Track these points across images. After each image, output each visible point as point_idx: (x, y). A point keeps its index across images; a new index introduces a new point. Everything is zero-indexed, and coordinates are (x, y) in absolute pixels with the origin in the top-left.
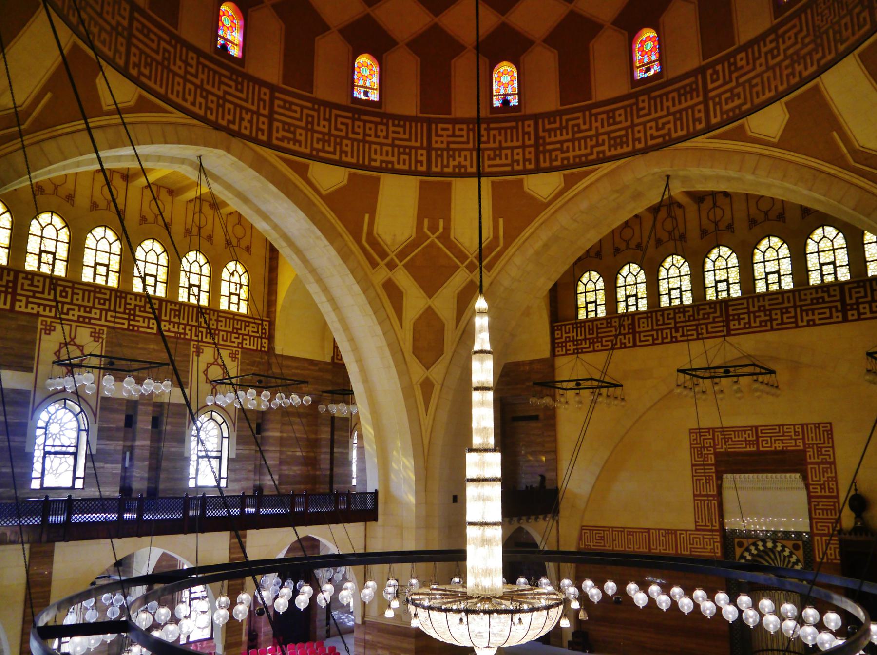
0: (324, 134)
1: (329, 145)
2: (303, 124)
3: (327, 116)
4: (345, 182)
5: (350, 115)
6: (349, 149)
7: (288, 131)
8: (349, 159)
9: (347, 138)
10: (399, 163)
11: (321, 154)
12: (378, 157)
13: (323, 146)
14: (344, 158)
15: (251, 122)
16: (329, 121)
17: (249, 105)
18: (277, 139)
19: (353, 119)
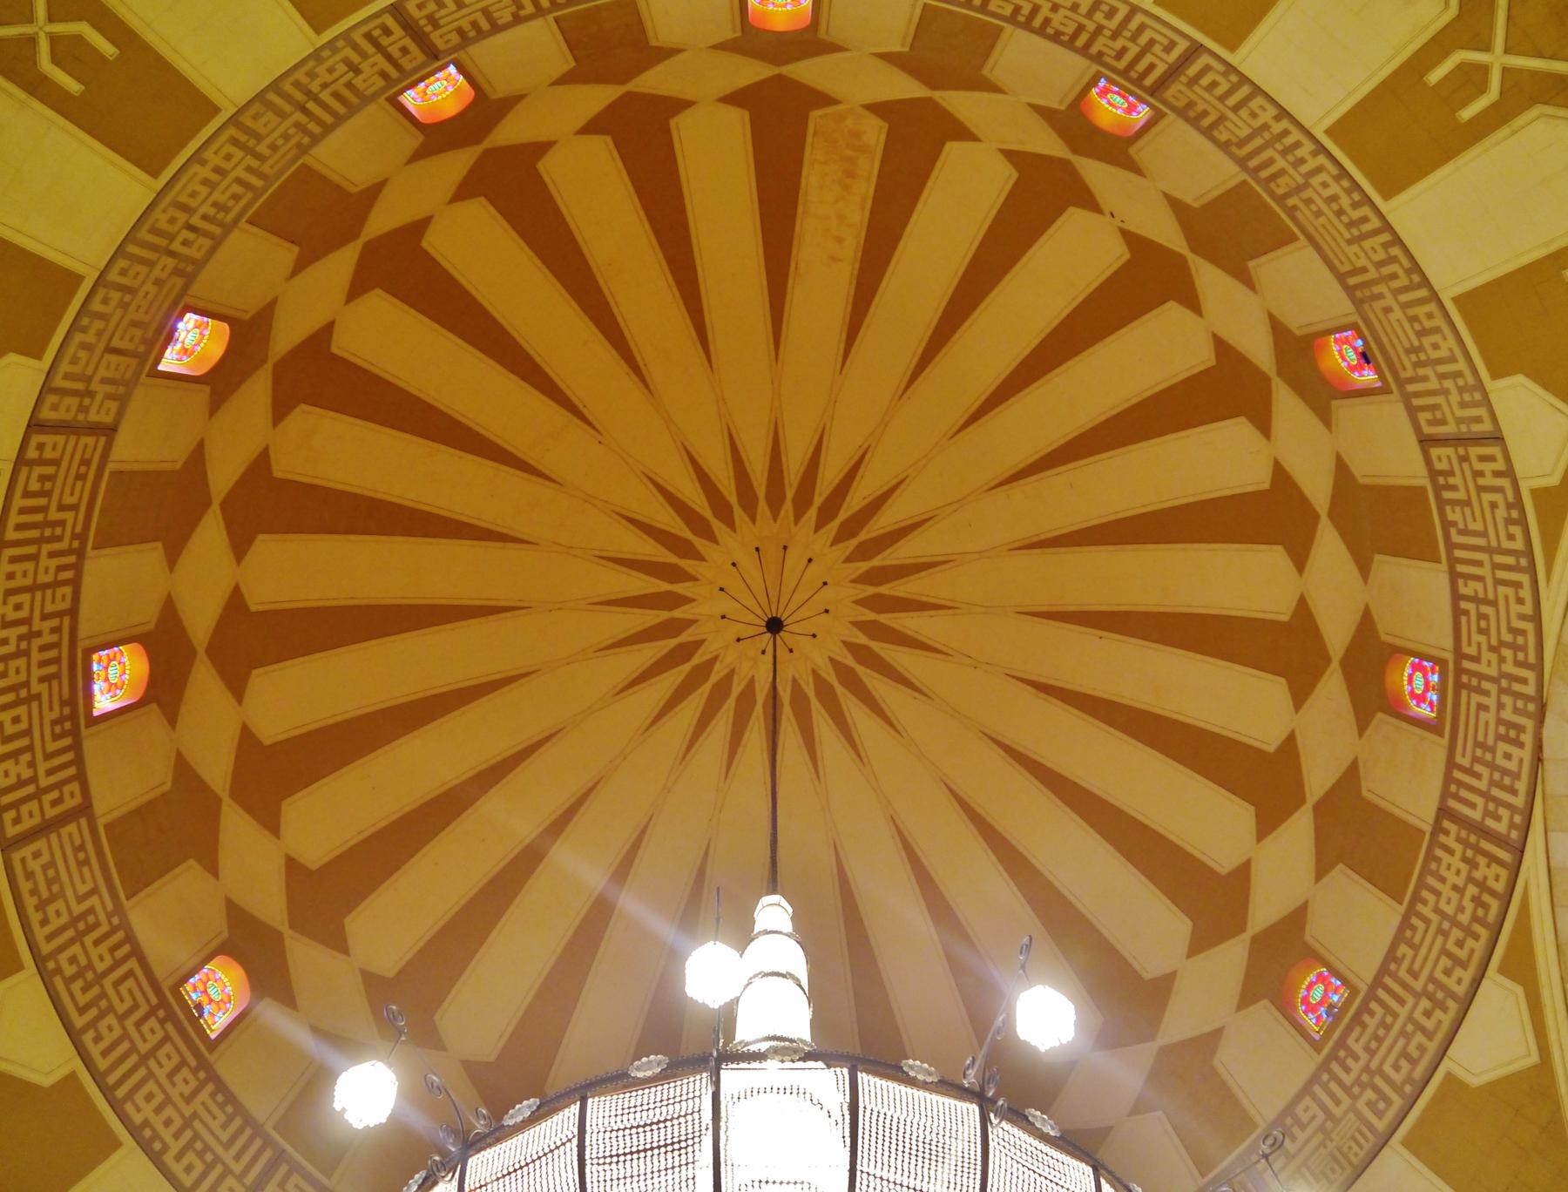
0: (90, 966)
1: (84, 990)
2: (78, 909)
3: (120, 953)
4: (47, 1081)
5: (154, 1000)
6: (108, 1039)
7: (49, 883)
8: (95, 1051)
9: (122, 1018)
10: (178, 1158)
11: (58, 982)
12: (148, 1111)
13: (75, 977)
14: (88, 1038)
15: (21, 783)
16: (117, 964)
17: (42, 767)
18: (23, 860)
19: (152, 1012)
